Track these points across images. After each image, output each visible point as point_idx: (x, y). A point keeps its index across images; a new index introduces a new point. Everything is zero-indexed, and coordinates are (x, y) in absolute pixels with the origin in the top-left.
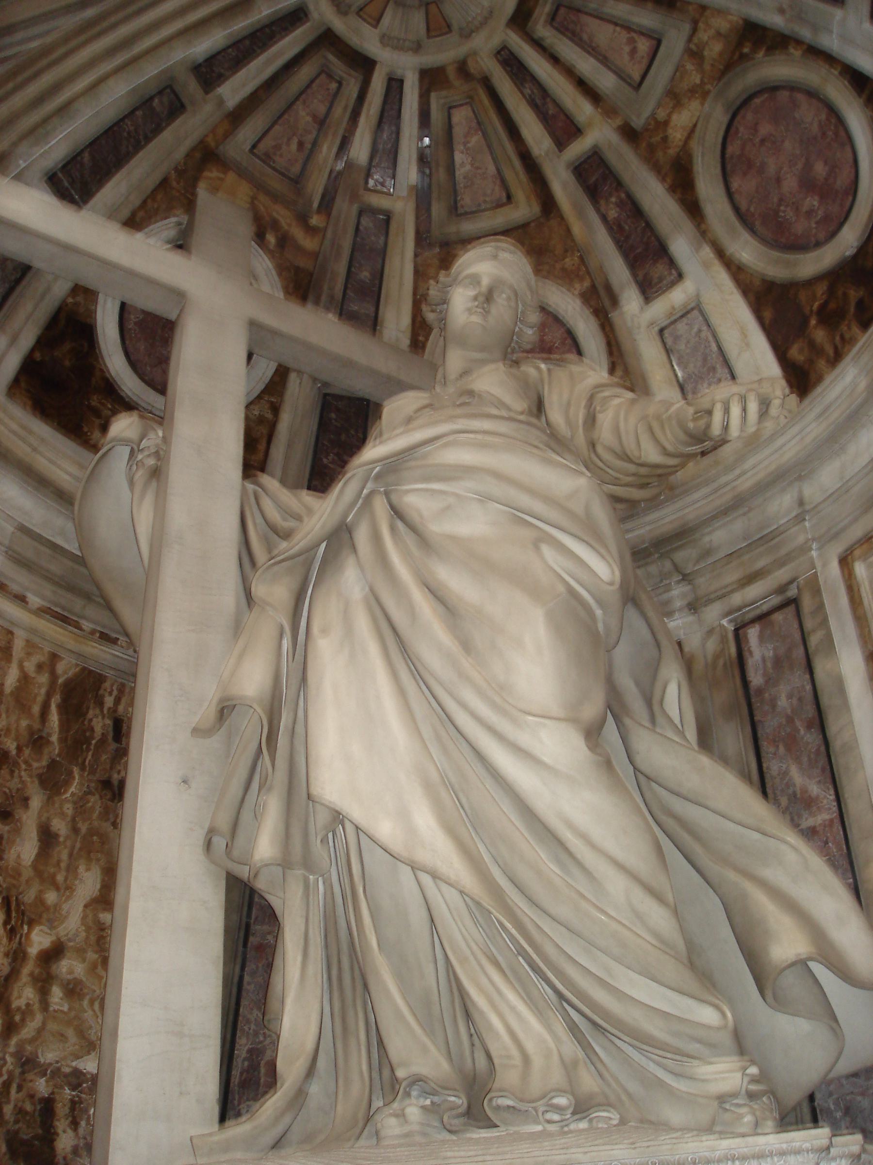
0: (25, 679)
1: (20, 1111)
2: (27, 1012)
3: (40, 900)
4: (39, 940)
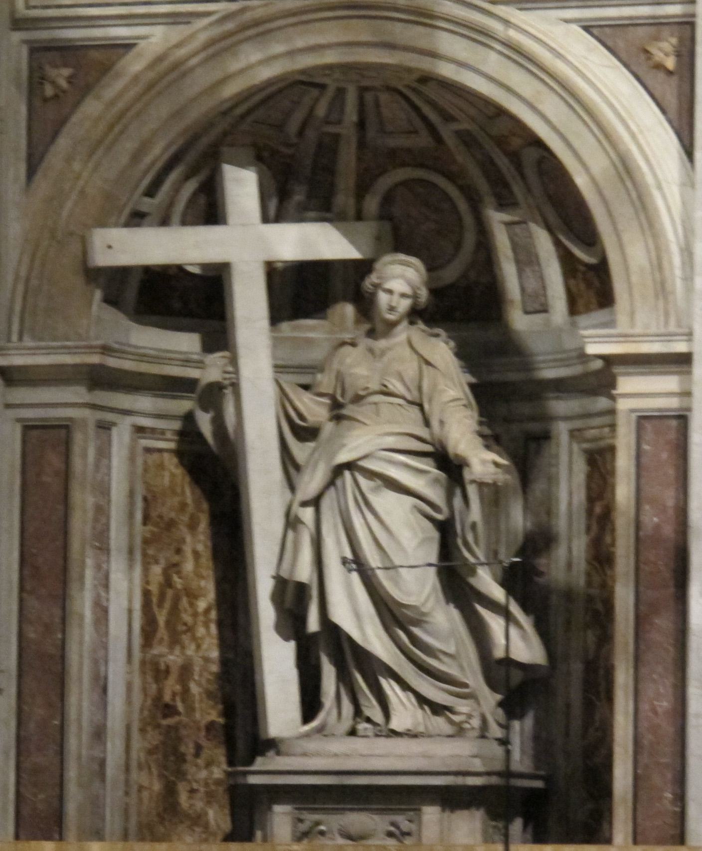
0: (173, 475)
1: (208, 681)
2: (202, 638)
3: (199, 586)
4: (202, 605)
